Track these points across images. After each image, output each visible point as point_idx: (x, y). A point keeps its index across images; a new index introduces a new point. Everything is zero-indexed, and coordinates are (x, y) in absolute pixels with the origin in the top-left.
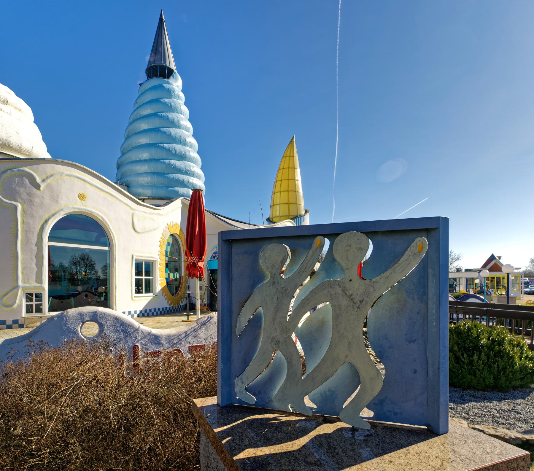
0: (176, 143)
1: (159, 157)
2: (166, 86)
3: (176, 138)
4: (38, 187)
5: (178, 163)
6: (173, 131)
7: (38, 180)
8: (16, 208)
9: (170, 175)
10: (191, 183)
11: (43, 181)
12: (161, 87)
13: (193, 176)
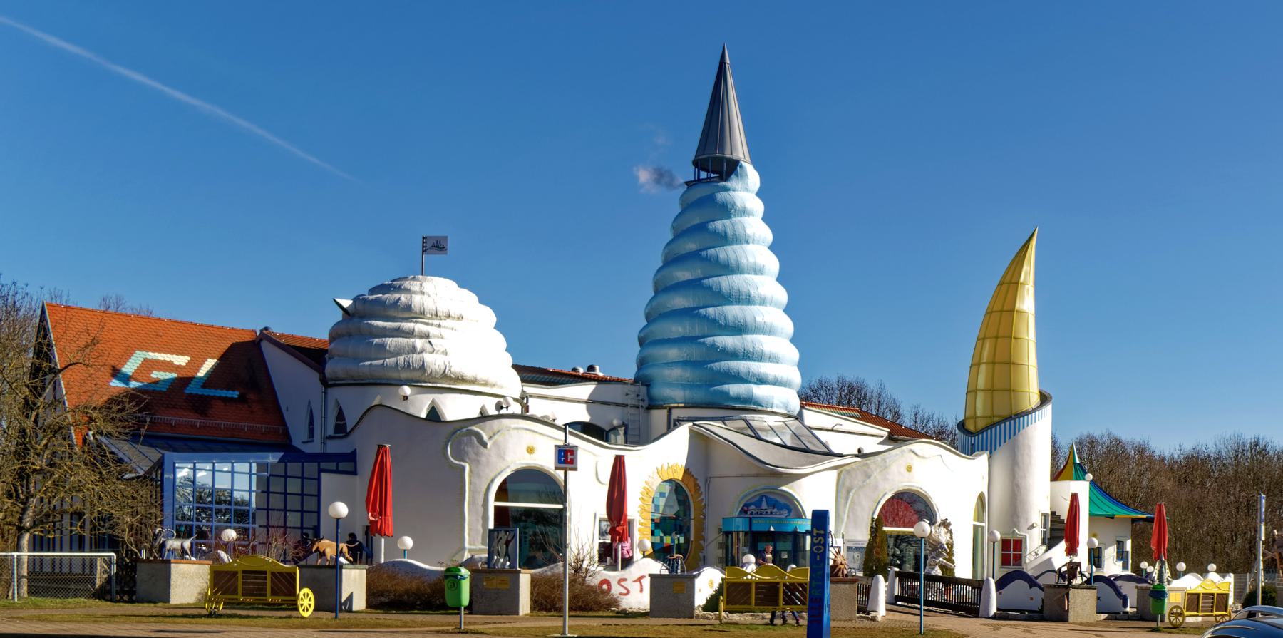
0: (731, 303)
1: (697, 332)
2: (721, 196)
3: (730, 295)
10: (754, 374)
12: (711, 199)
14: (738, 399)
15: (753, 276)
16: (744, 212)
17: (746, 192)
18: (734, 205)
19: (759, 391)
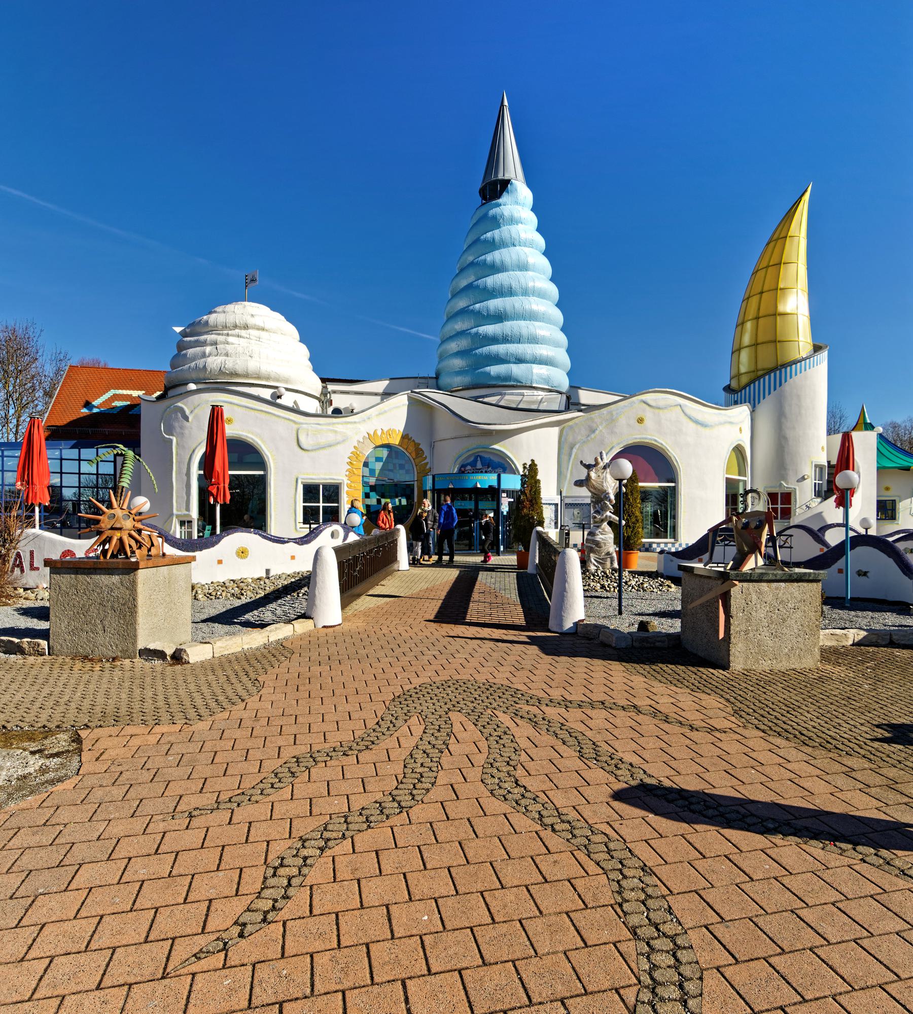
0: (495, 297)
3: (494, 290)
4: (187, 419)
5: (489, 329)
6: (491, 281)
7: (187, 412)
8: (171, 441)
9: (477, 351)
10: (512, 354)
11: (191, 412)
13: (519, 342)
14: (498, 377)
15: (518, 273)
16: (513, 221)
17: (519, 205)
18: (502, 216)
19: (517, 370)
